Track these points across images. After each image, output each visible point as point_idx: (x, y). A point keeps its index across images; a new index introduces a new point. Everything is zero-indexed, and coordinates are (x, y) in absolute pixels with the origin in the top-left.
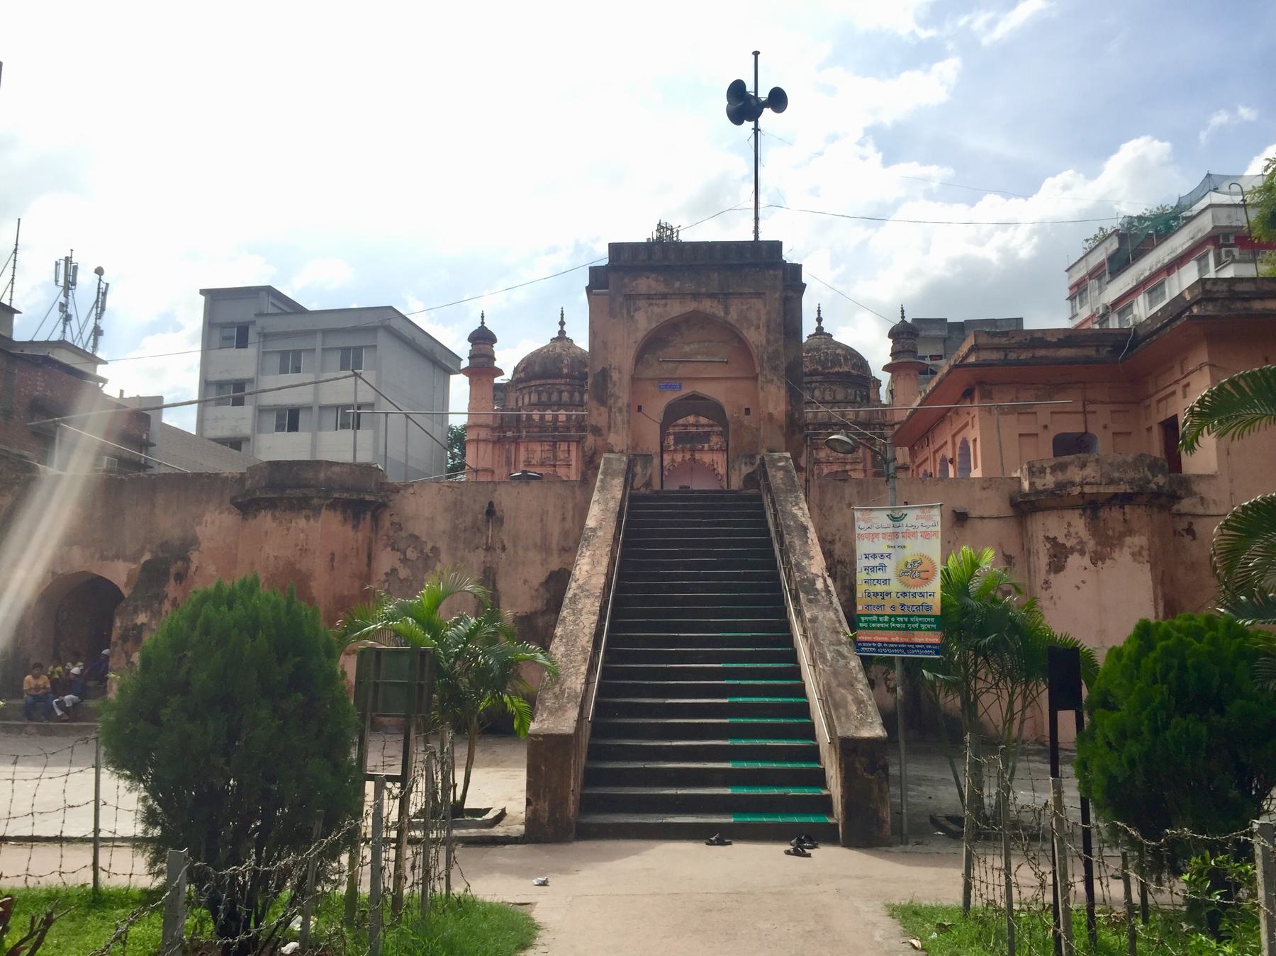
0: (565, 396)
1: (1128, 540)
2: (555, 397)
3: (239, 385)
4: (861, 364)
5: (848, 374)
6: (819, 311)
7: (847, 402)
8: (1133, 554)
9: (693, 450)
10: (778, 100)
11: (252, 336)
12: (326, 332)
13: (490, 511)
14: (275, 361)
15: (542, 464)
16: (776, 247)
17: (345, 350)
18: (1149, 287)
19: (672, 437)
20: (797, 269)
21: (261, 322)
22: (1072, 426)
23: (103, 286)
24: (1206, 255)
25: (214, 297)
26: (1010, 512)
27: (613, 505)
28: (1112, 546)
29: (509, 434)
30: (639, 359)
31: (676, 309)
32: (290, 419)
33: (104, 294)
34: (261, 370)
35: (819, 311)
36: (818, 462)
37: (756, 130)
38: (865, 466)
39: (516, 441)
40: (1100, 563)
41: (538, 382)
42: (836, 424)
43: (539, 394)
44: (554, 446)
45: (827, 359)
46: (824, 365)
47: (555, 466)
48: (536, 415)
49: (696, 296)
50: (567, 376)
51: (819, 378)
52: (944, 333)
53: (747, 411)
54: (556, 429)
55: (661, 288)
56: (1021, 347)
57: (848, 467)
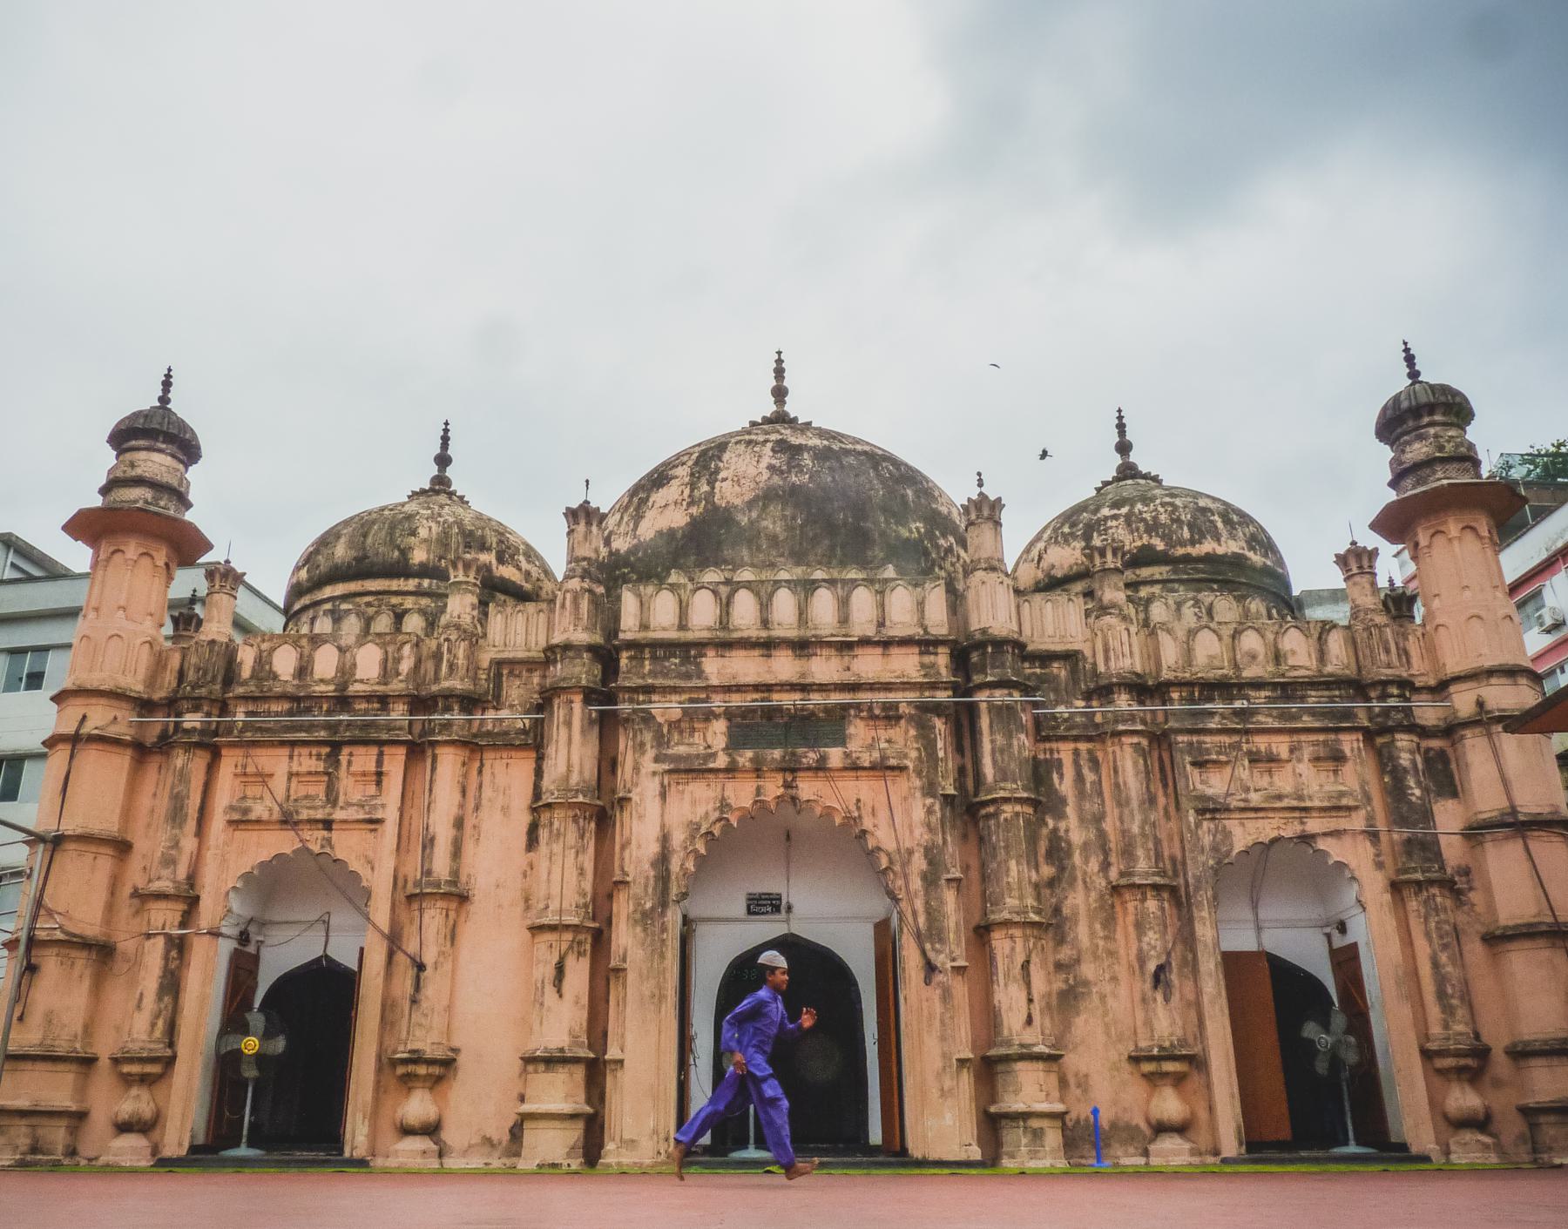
5: (1237, 561)
6: (1121, 427)
9: (791, 768)
15: (287, 821)
19: (720, 726)
29: (192, 720)
35: (1121, 427)
36: (1211, 809)
38: (1370, 819)
39: (210, 745)
42: (1258, 685)
44: (333, 759)
45: (1178, 521)
47: (328, 824)
48: (285, 663)
54: (343, 701)
57: (1314, 825)
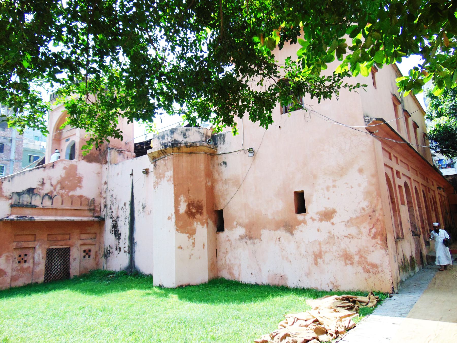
8: (168, 181)
28: (161, 178)
40: (156, 188)
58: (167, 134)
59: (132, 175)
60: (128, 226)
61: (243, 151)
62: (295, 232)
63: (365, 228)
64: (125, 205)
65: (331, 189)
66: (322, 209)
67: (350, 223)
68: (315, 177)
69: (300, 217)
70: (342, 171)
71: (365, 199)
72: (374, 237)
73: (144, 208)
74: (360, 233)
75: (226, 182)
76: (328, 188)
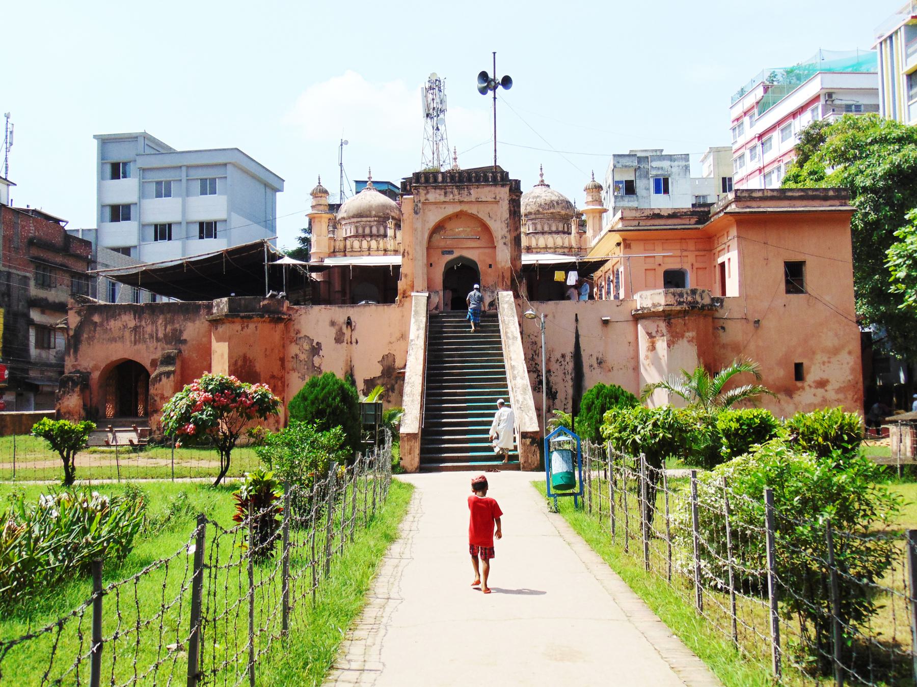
0: (374, 230)
1: (687, 334)
2: (367, 231)
3: (127, 207)
4: (568, 205)
7: (557, 232)
8: (689, 341)
10: (507, 82)
11: (132, 169)
12: (188, 167)
13: (349, 323)
14: (153, 187)
16: (505, 175)
17: (203, 181)
18: (782, 126)
20: (518, 183)
21: (137, 158)
22: (674, 265)
23: (9, 126)
24: (817, 108)
25: (105, 142)
26: (631, 318)
27: (423, 325)
28: (678, 337)
30: (430, 237)
31: (450, 210)
32: (163, 232)
33: (11, 132)
34: (143, 195)
37: (495, 98)
41: (355, 220)
42: (550, 248)
43: (357, 227)
46: (544, 209)
49: (461, 202)
50: (375, 216)
51: (541, 216)
52: (635, 164)
53: (490, 266)
55: (442, 198)
56: (648, 217)
58: (687, 293)
59: (577, 320)
60: (570, 383)
61: (744, 321)
62: (794, 396)
63: (850, 395)
64: (563, 356)
65: (827, 364)
66: (818, 378)
67: (838, 391)
68: (814, 353)
69: (799, 384)
70: (836, 351)
71: (851, 374)
72: (856, 401)
73: (600, 363)
74: (846, 398)
75: (724, 346)
76: (824, 363)
